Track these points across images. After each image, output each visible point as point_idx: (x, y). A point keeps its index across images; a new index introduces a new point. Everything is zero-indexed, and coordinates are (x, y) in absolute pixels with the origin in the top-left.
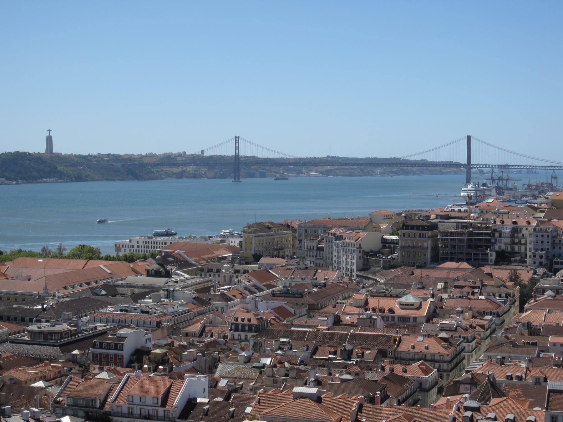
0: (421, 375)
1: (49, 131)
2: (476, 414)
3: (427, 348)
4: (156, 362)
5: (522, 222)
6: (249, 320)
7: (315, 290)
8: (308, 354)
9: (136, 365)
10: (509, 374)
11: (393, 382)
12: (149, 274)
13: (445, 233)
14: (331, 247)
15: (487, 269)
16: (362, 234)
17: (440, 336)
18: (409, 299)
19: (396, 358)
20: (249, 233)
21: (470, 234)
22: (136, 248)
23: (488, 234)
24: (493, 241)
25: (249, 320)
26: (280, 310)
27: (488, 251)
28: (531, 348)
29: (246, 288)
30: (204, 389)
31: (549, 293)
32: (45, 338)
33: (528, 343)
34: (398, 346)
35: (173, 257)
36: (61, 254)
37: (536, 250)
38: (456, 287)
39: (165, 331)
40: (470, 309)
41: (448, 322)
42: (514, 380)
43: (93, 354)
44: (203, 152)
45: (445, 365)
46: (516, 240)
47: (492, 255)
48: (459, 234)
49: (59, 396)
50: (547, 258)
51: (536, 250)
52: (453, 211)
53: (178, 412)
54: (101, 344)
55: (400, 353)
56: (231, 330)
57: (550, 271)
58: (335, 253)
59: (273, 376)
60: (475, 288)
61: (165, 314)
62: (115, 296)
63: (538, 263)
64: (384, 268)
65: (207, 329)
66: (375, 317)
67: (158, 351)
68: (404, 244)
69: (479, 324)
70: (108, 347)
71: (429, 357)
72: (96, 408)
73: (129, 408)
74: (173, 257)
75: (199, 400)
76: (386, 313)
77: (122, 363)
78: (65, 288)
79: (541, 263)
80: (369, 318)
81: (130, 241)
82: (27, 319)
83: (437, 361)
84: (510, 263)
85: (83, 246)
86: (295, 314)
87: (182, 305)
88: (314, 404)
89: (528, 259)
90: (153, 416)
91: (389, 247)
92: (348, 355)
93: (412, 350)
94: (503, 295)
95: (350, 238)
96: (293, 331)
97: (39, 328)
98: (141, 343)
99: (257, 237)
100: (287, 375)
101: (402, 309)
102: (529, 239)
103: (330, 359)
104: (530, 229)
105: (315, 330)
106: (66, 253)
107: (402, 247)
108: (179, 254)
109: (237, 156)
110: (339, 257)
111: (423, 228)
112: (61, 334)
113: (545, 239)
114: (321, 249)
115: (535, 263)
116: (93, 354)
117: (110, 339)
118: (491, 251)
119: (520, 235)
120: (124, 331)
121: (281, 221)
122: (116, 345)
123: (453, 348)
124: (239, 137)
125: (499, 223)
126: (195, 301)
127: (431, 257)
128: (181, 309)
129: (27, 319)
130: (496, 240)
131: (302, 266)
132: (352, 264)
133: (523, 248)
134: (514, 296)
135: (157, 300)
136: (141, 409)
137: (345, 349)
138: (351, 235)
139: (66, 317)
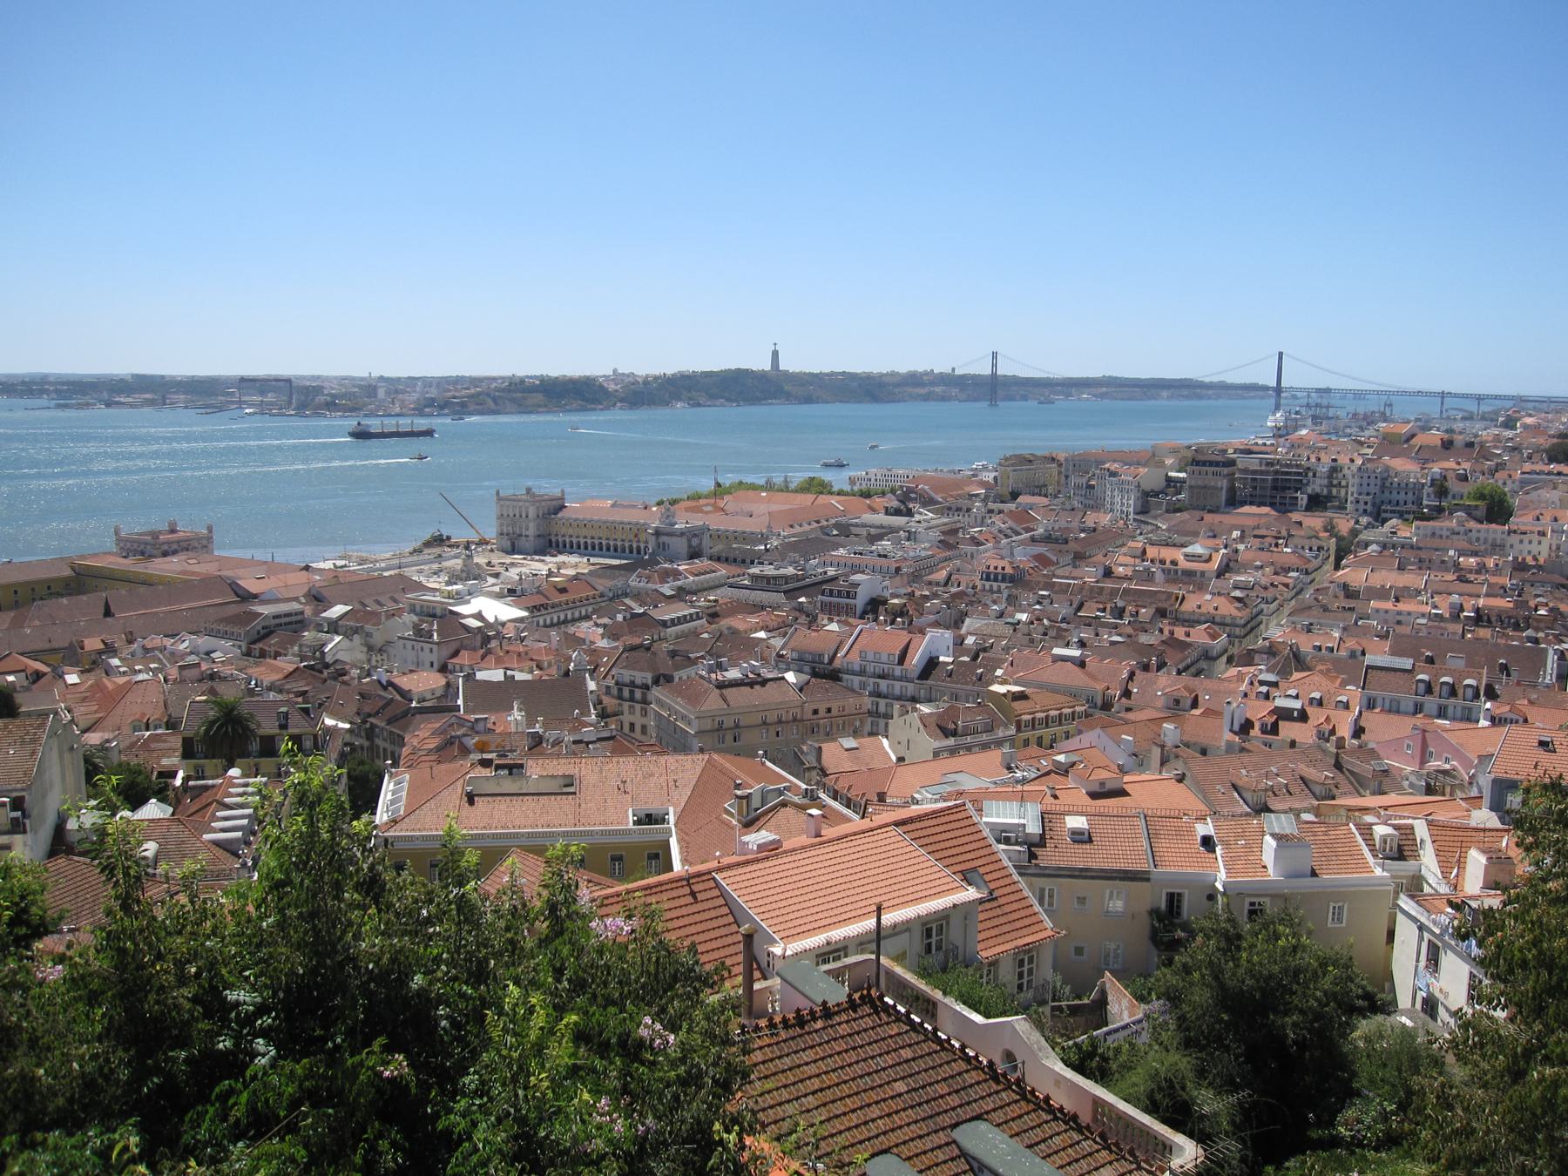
0: (1208, 641)
2: (1272, 690)
3: (1216, 609)
5: (1343, 460)
6: (1003, 569)
7: (1083, 535)
8: (1071, 610)
12: (887, 512)
13: (1245, 471)
15: (1295, 516)
16: (1143, 470)
18: (1197, 549)
19: (1177, 620)
21: (1277, 472)
25: (1003, 569)
26: (1042, 560)
28: (1348, 614)
29: (1000, 531)
31: (1374, 547)
32: (768, 583)
36: (787, 487)
37: (1360, 494)
38: (1255, 536)
40: (1272, 563)
44: (953, 369)
45: (1237, 630)
46: (1335, 482)
47: (1303, 499)
48: (1262, 473)
49: (782, 649)
50: (1374, 504)
51: (1360, 494)
52: (1256, 444)
54: (831, 591)
55: (1183, 613)
58: (1109, 493)
60: (1279, 538)
64: (1167, 511)
67: (896, 601)
68: (1193, 483)
70: (840, 594)
71: (1218, 619)
78: (792, 526)
79: (1365, 511)
80: (1147, 570)
82: (748, 561)
83: (1227, 625)
84: (1325, 509)
85: (812, 479)
87: (925, 549)
88: (1077, 669)
89: (1349, 505)
92: (1120, 613)
94: (1315, 548)
98: (877, 592)
100: (1045, 634)
103: (1097, 617)
104: (1354, 468)
105: (1080, 582)
106: (792, 486)
107: (1191, 487)
109: (994, 375)
110: (1112, 497)
111: (1217, 464)
112: (786, 579)
114: (1092, 487)
117: (842, 586)
119: (1340, 475)
120: (857, 577)
121: (1046, 453)
122: (848, 592)
123: (1248, 610)
125: (1313, 460)
127: (1227, 500)
128: (923, 554)
129: (748, 561)
133: (1343, 492)
135: (897, 542)
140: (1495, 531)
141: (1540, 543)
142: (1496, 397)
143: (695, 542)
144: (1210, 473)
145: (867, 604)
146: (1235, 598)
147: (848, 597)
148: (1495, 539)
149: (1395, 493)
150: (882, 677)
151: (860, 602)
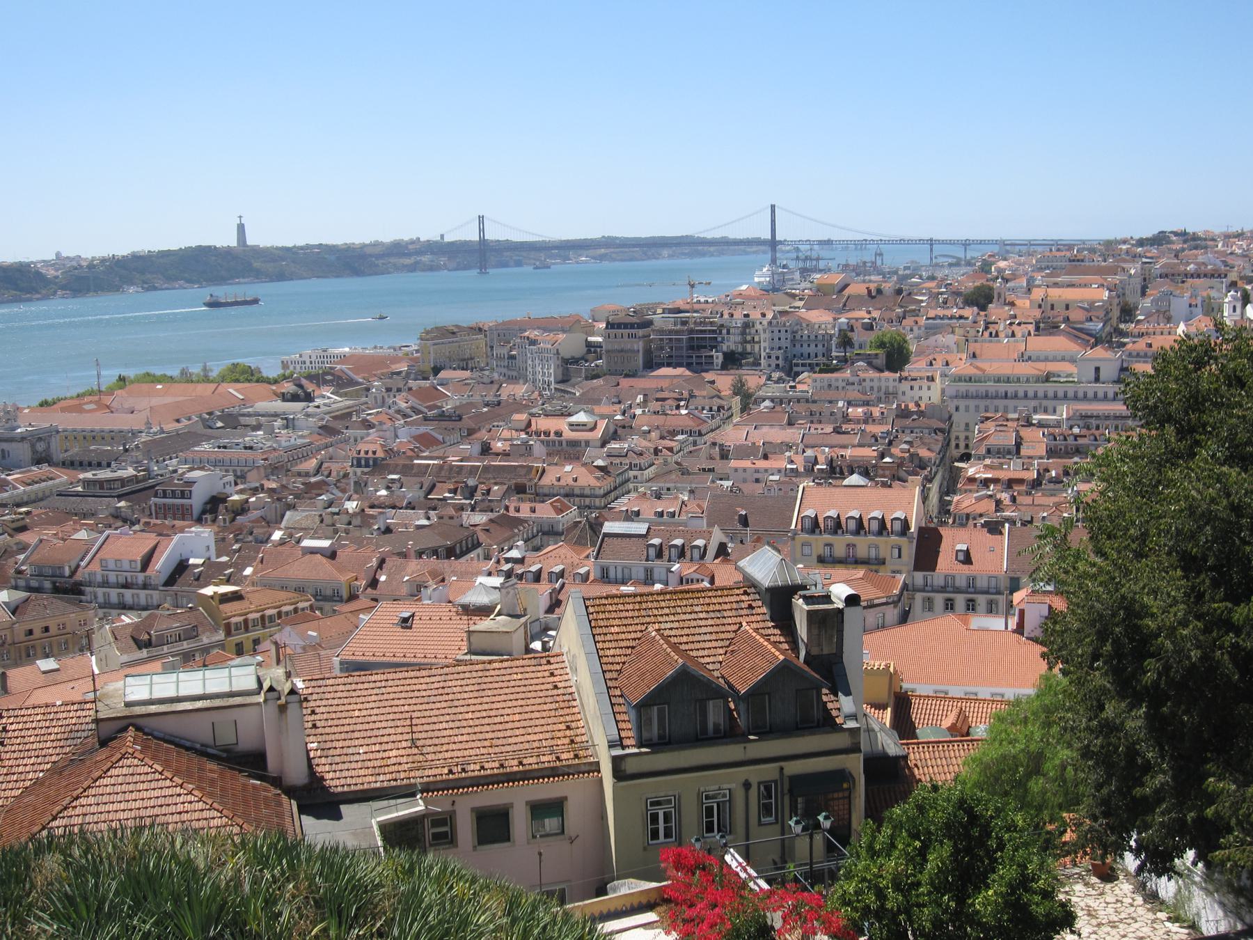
0: (553, 515)
1: (240, 217)
2: (516, 566)
3: (575, 480)
4: (233, 512)
5: (755, 315)
6: (374, 453)
7: (485, 409)
8: (421, 494)
9: (208, 516)
10: (660, 510)
11: (501, 526)
12: (284, 398)
13: (661, 332)
15: (709, 376)
16: (562, 336)
18: (581, 417)
19: (537, 495)
20: (427, 340)
21: (691, 331)
22: (308, 364)
23: (714, 331)
24: (719, 339)
25: (374, 453)
27: (713, 353)
28: (705, 476)
30: (208, 547)
31: (767, 403)
32: (102, 488)
33: (704, 470)
34: (540, 479)
35: (333, 375)
36: (206, 376)
37: (772, 349)
38: (658, 400)
39: (262, 470)
40: (658, 427)
41: (617, 446)
42: (665, 517)
43: (156, 504)
44: (442, 236)
45: (597, 500)
46: (749, 338)
47: (718, 358)
48: (677, 332)
49: (22, 564)
50: (786, 359)
51: (772, 349)
52: (699, 302)
53: (163, 578)
54: (164, 491)
55: (542, 487)
56: (352, 466)
57: (789, 375)
58: (530, 362)
59: (333, 525)
60: (681, 400)
61: (275, 449)
62: (236, 428)
63: (773, 366)
64: (587, 378)
65: (325, 465)
66: (531, 443)
67: (236, 497)
68: (610, 347)
70: (174, 496)
71: (577, 491)
72: (64, 577)
73: (103, 576)
74: (333, 375)
75: (192, 561)
76: (552, 436)
77: (192, 514)
78: (178, 421)
79: (777, 365)
80: (525, 443)
81: (301, 356)
82: (104, 463)
83: (587, 496)
84: (740, 366)
85: (236, 365)
86: (444, 442)
87: (302, 437)
88: (324, 560)
89: (762, 361)
90: (132, 584)
91: (595, 352)
92: (471, 492)
93: (556, 483)
94: (715, 408)
95: (546, 340)
97: (94, 475)
98: (217, 488)
100: (349, 523)
101: (572, 430)
102: (763, 336)
103: (445, 499)
104: (765, 322)
106: (214, 374)
107: (608, 351)
110: (534, 367)
111: (632, 326)
112: (123, 482)
113: (783, 335)
114: (513, 357)
115: (769, 366)
116: (156, 504)
117: (176, 485)
118: (717, 352)
119: (753, 331)
120: (196, 474)
121: (472, 323)
122: (182, 492)
123: (610, 479)
125: (726, 316)
126: (321, 431)
127: (644, 363)
128: (300, 442)
129: (104, 463)
130: (723, 339)
131: (486, 380)
132: (550, 375)
133: (757, 347)
134: (730, 408)
135: (271, 432)
136: (117, 576)
137: (467, 486)
138: (548, 338)
139: (134, 459)
140: (887, 380)
141: (929, 388)
142: (981, 242)
143: (40, 447)
144: (626, 336)
145: (206, 503)
146: (597, 467)
147: (183, 497)
148: (887, 387)
149: (805, 345)
150: (126, 586)
151: (198, 499)
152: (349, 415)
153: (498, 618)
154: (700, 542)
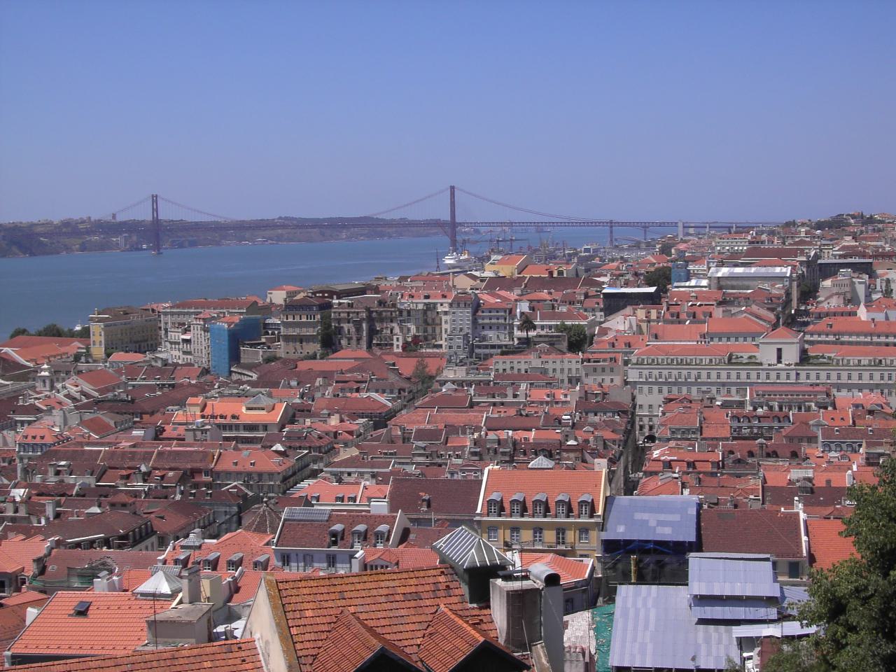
6: (42, 438)
14: (199, 336)
17: (274, 448)
29: (68, 396)
44: (114, 216)
60: (362, 382)
69: (346, 430)
96: (84, 451)
99: (108, 326)
108: (5, 353)
124: (156, 196)
133: (438, 330)
142: (661, 225)
146: (277, 452)
152: (16, 398)
153: (180, 607)
154: (383, 528)
